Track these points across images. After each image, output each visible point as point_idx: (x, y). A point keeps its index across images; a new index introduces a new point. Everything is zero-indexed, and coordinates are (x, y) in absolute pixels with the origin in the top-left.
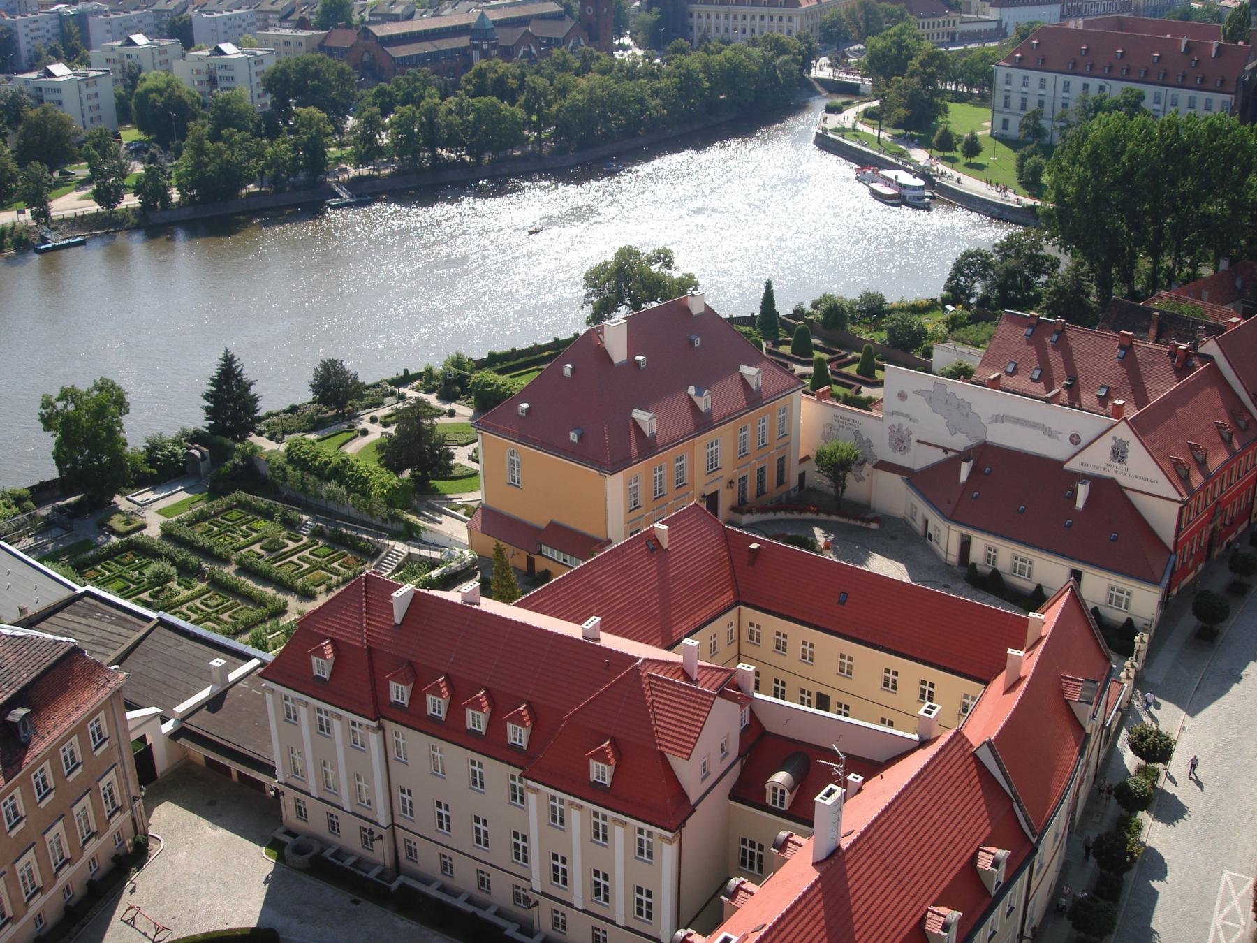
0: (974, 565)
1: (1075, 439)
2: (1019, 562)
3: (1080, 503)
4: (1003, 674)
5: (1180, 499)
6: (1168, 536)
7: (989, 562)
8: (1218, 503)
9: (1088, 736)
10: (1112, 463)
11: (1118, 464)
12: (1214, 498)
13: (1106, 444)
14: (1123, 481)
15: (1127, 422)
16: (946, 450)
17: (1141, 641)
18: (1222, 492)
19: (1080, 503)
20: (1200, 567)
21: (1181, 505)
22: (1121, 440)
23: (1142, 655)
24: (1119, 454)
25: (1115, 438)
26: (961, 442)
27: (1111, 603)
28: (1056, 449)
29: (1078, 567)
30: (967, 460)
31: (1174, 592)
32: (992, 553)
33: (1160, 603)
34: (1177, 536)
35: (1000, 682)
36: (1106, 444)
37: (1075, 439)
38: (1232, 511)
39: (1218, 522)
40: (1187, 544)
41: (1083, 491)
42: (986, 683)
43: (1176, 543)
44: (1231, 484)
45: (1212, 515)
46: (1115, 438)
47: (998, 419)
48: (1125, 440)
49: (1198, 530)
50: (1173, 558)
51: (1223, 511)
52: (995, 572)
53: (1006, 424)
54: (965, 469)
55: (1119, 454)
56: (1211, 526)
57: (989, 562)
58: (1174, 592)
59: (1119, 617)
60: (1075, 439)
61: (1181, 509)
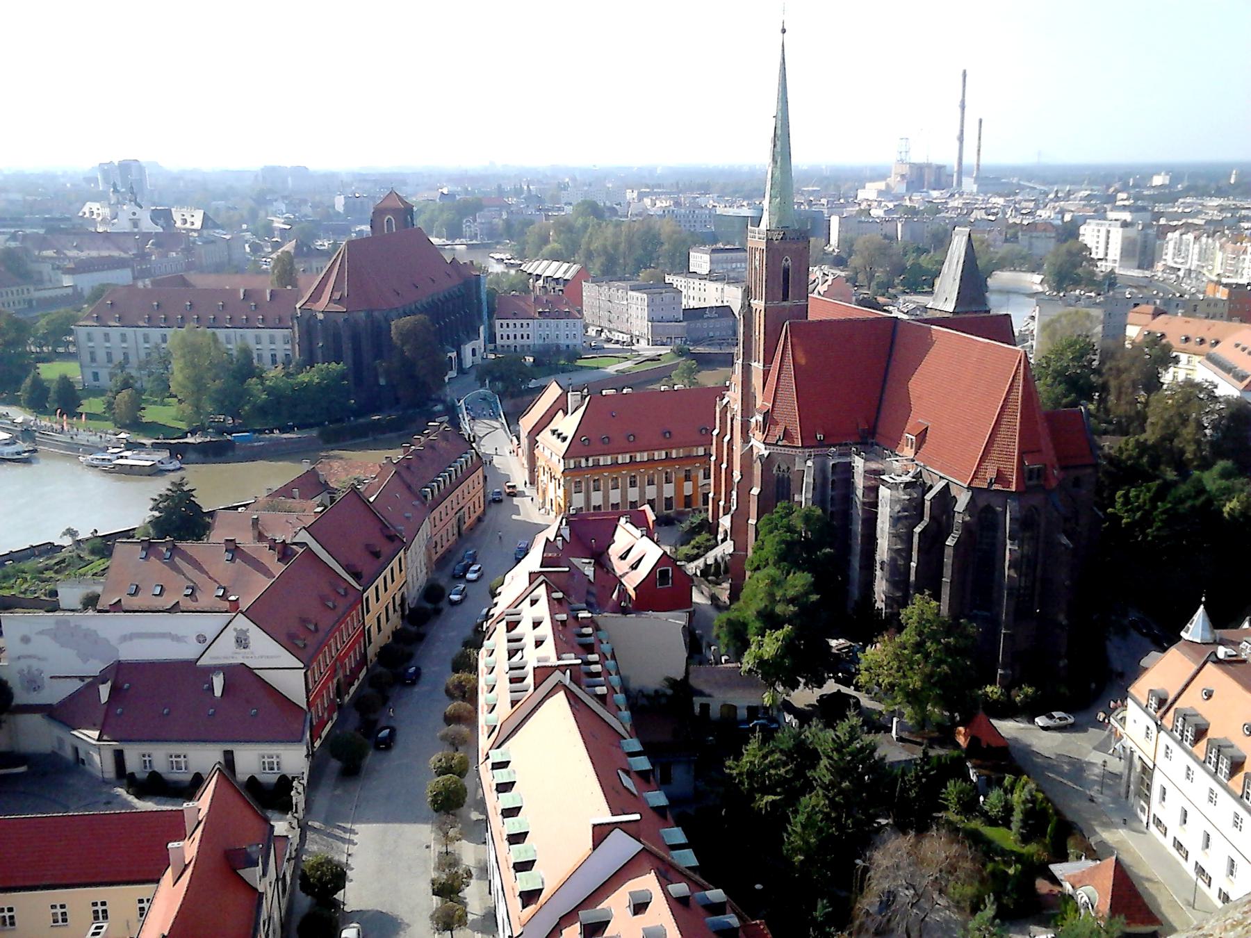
0: (132, 774)
1: (201, 639)
2: (174, 759)
3: (218, 692)
4: (170, 869)
5: (302, 666)
6: (300, 699)
7: (145, 767)
8: (336, 660)
9: (261, 895)
10: (238, 650)
11: (244, 650)
12: (333, 657)
13: (229, 636)
14: (251, 663)
15: (242, 613)
16: (82, 678)
17: (298, 797)
18: (338, 650)
19: (218, 692)
20: (335, 716)
21: (304, 671)
22: (241, 630)
23: (301, 806)
24: (242, 642)
25: (235, 630)
26: (95, 667)
27: (264, 769)
28: (186, 651)
29: (228, 747)
30: (103, 683)
31: (317, 744)
32: (147, 758)
33: (307, 756)
34: (308, 697)
35: (169, 875)
36: (230, 635)
37: (201, 639)
38: (350, 663)
39: (340, 675)
40: (318, 701)
41: (218, 682)
42: (158, 881)
43: (308, 701)
44: (344, 642)
45: (334, 671)
46: (235, 630)
47: (126, 638)
48: (244, 629)
49: (325, 686)
50: (309, 717)
51: (343, 666)
52: (155, 776)
53: (135, 641)
54: (104, 691)
55: (242, 642)
56: (335, 681)
57: (145, 767)
58: (317, 744)
59: (270, 778)
60: (201, 639)
61: (305, 674)
